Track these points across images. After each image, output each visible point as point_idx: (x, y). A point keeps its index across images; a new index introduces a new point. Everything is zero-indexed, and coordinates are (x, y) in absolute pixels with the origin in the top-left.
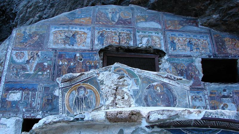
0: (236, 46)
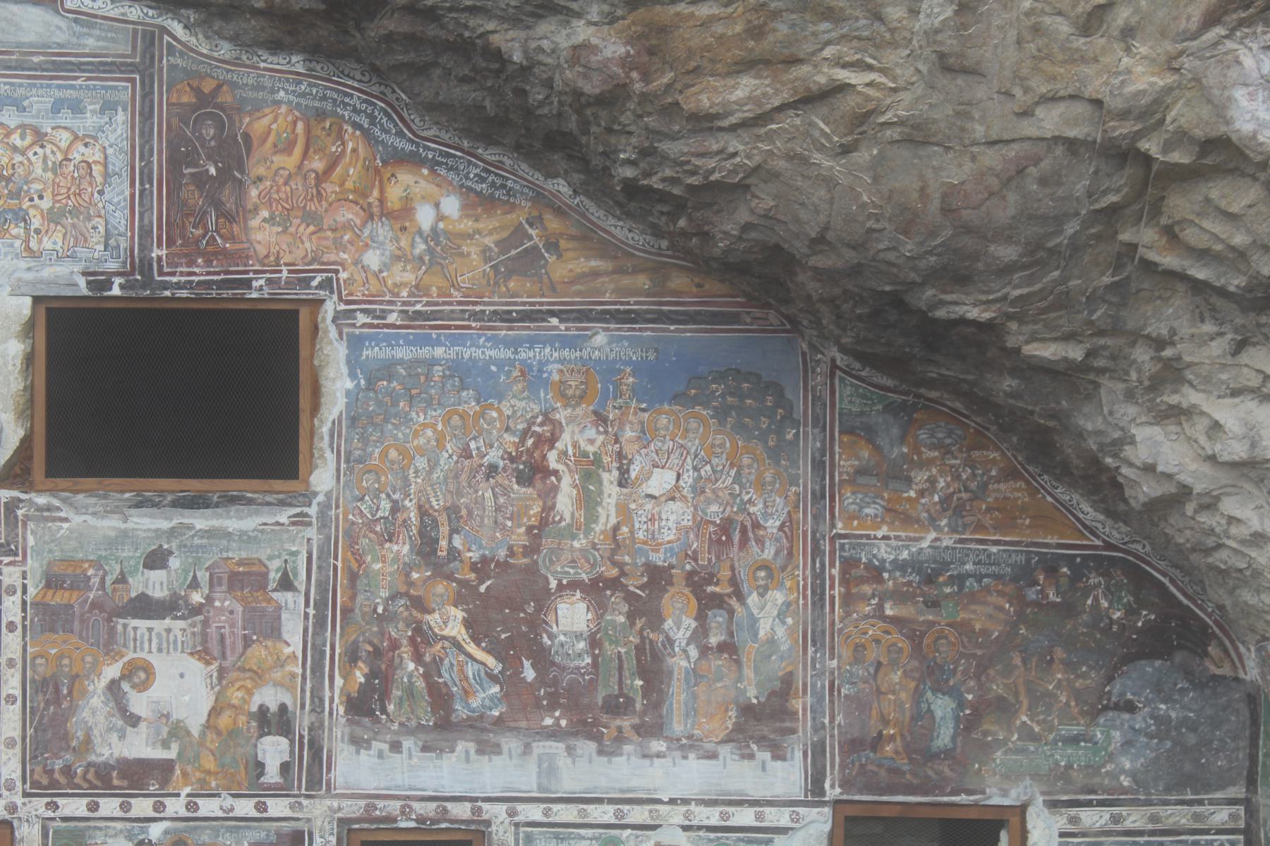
0: (330, 188)
